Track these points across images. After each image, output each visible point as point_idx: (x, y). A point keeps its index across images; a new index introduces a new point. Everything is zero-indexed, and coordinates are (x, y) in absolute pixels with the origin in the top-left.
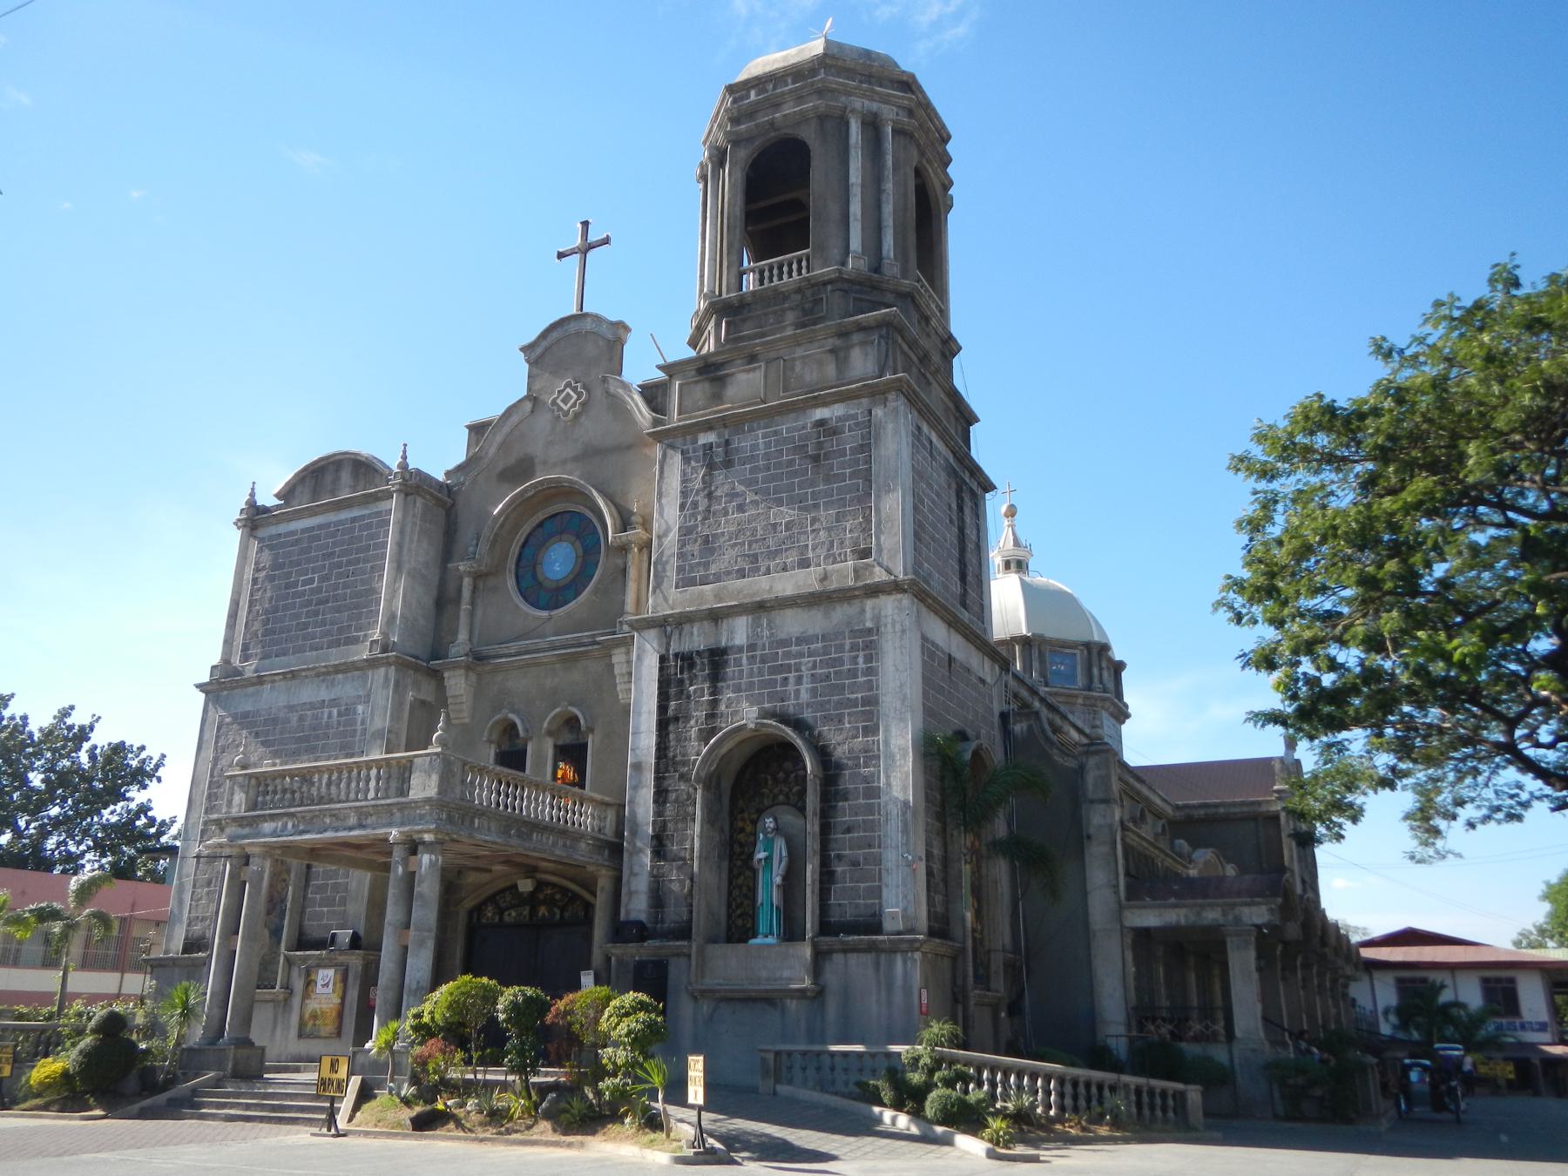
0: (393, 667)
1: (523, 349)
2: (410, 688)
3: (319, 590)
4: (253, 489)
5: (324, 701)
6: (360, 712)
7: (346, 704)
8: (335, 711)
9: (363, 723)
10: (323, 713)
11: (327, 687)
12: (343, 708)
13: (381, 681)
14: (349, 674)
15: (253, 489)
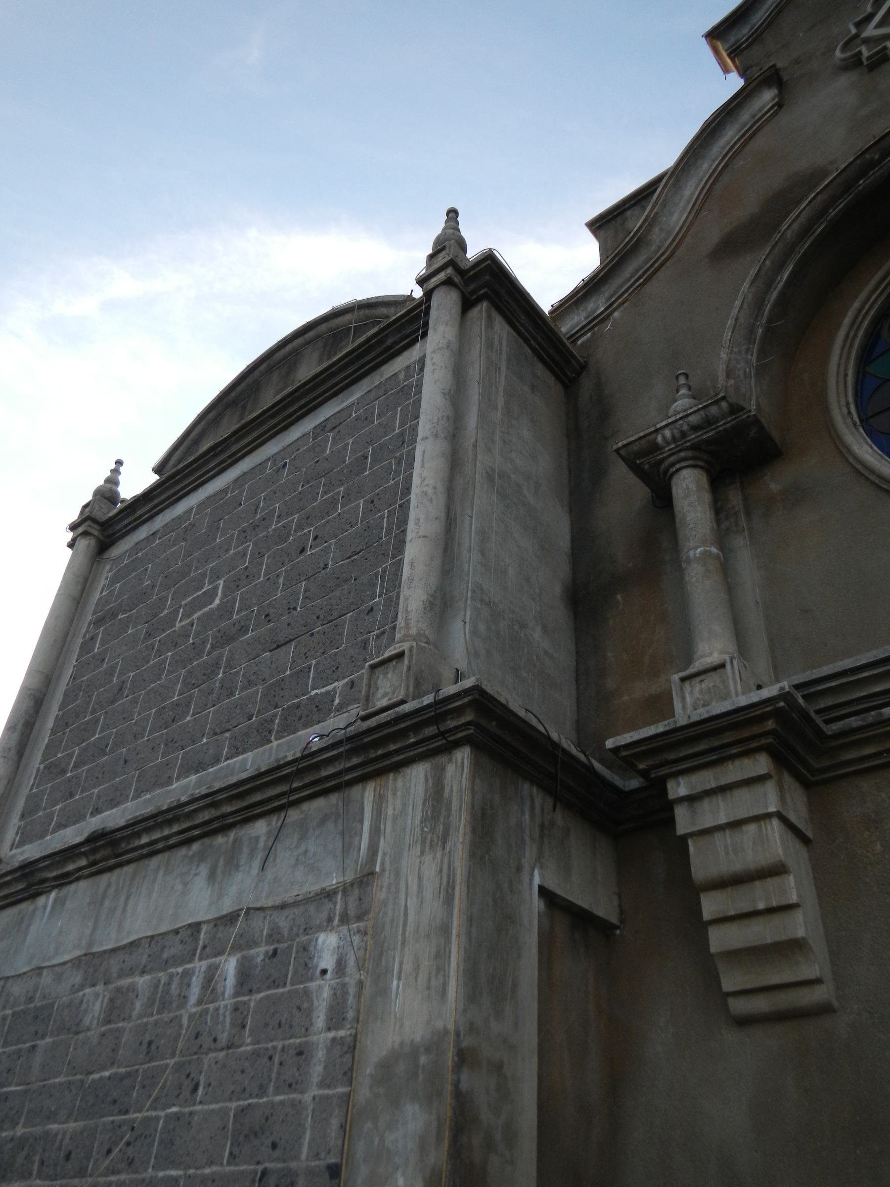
0: (463, 755)
1: (715, 35)
2: (530, 853)
3: (225, 610)
4: (116, 472)
5: (196, 927)
6: (327, 961)
7: (274, 935)
8: (230, 966)
9: (335, 1019)
10: (187, 975)
11: (212, 877)
12: (260, 952)
13: (415, 817)
14: (294, 815)
15: (116, 472)
